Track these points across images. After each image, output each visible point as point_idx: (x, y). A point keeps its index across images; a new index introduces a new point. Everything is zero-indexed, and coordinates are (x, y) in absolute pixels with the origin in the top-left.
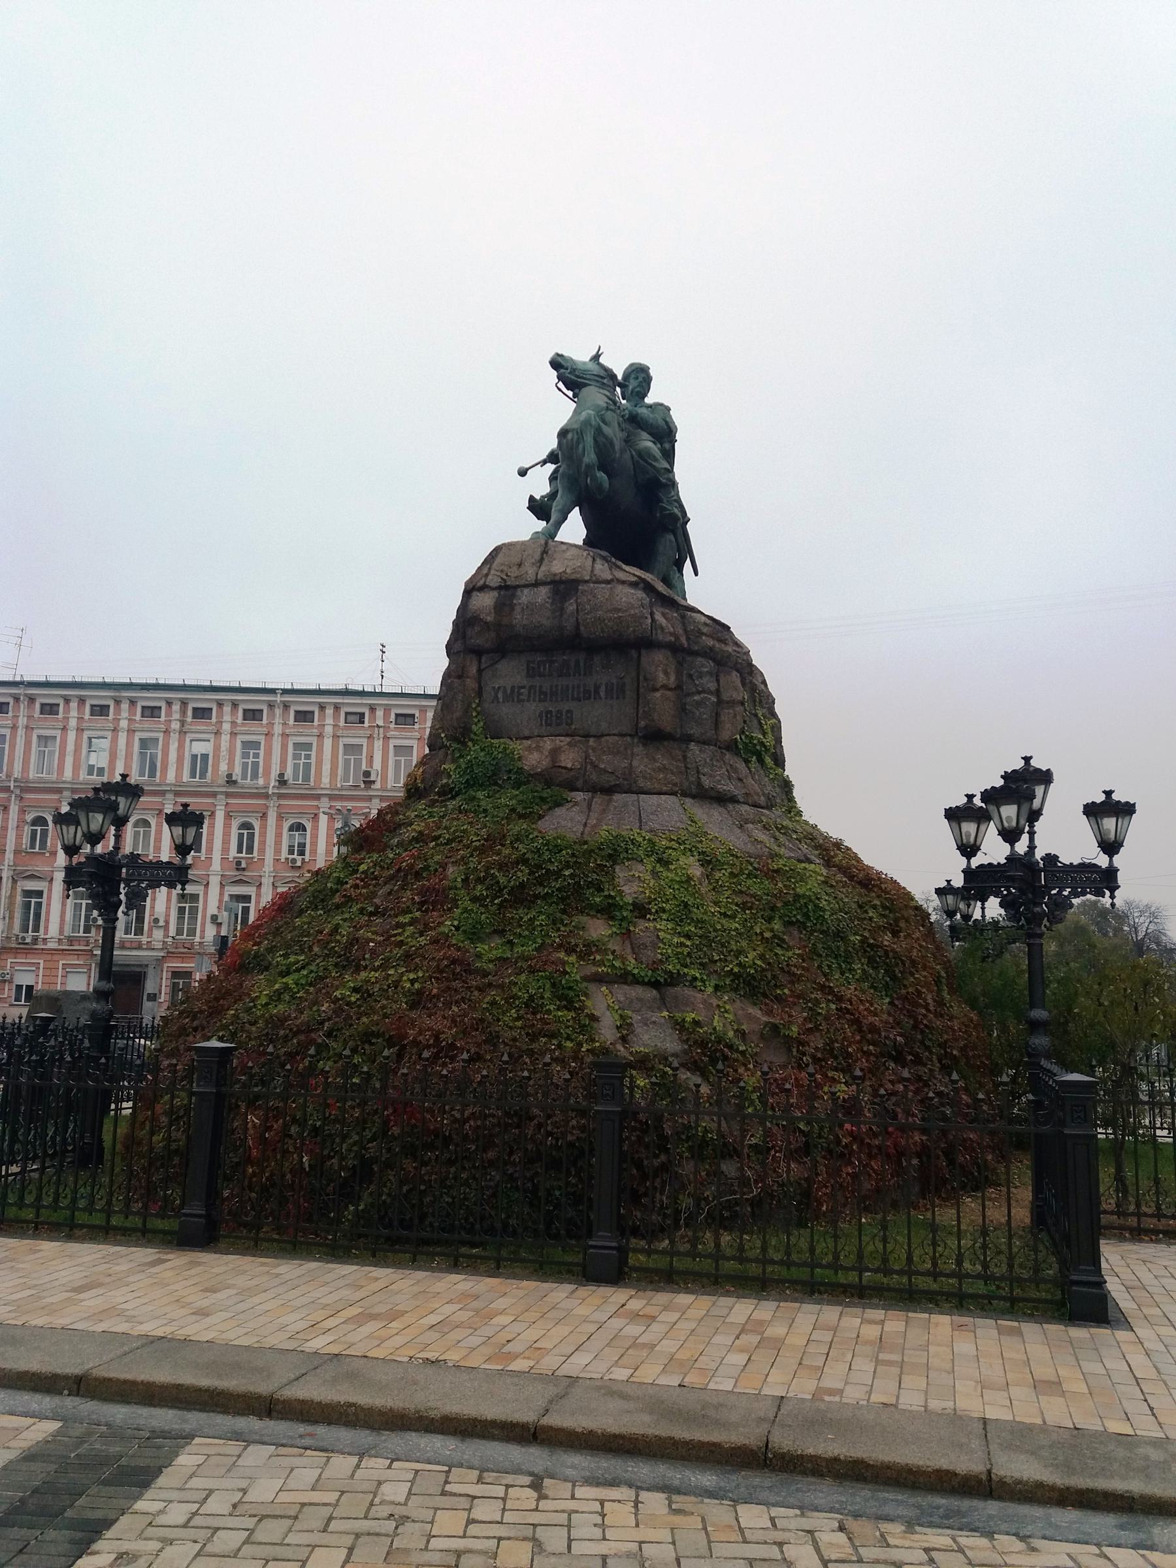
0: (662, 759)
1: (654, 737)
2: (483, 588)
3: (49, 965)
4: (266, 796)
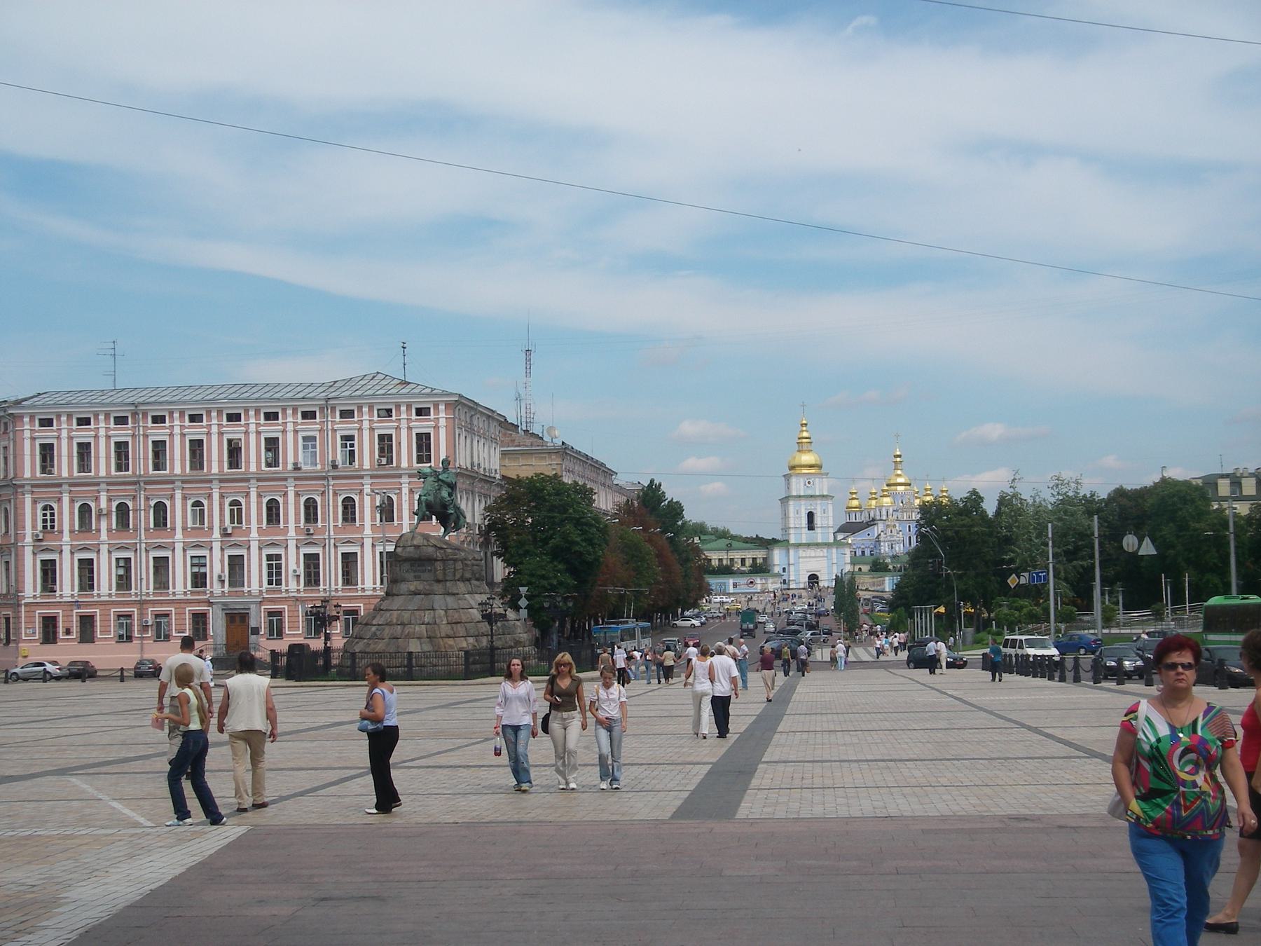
0: (440, 586)
1: (438, 581)
2: (399, 547)
3: (180, 611)
4: (324, 478)
